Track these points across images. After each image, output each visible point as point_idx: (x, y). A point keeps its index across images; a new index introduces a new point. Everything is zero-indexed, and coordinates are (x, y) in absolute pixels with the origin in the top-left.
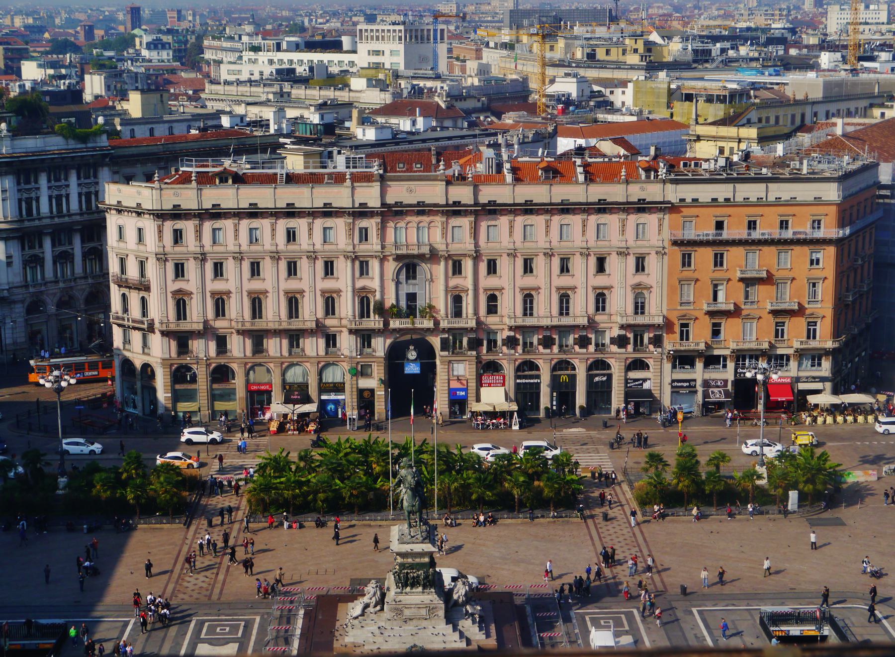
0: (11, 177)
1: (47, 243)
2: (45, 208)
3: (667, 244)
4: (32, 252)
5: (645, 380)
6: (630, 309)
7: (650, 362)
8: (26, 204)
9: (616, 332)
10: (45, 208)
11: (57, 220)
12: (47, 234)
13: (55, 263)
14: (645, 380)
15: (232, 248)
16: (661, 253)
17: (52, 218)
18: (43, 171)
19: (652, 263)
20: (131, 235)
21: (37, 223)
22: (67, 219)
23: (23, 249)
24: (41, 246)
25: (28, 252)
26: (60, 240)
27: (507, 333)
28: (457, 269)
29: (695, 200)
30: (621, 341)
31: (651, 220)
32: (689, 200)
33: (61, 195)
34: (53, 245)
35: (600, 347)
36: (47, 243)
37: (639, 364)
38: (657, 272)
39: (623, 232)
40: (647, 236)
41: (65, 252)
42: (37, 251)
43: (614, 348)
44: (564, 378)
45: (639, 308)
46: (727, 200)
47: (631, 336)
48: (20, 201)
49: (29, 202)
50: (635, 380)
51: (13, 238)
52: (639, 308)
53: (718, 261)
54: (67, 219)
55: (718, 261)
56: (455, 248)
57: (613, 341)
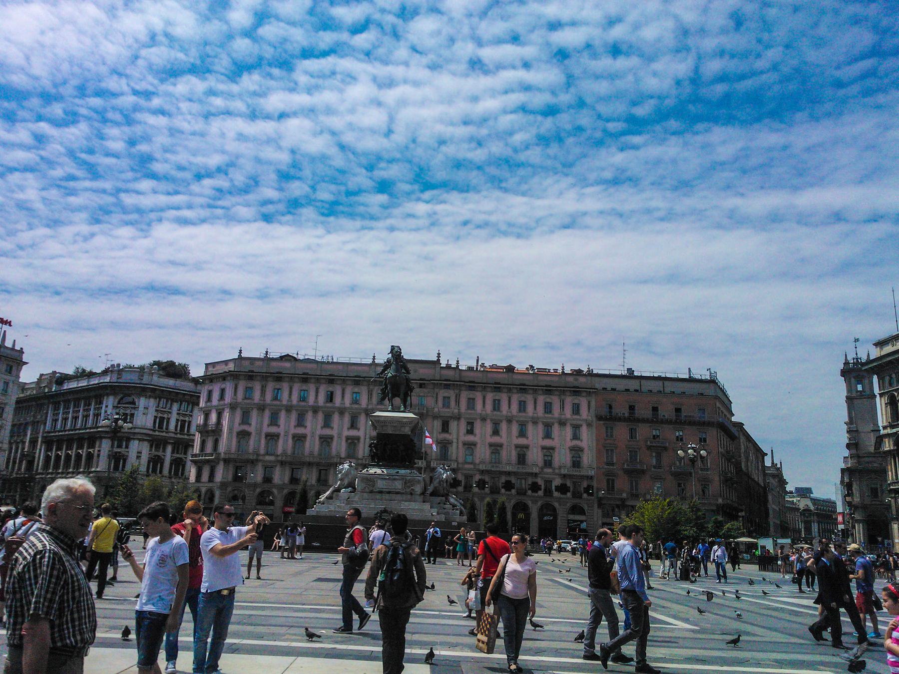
0: (152, 400)
1: (169, 449)
2: (172, 427)
3: (594, 419)
4: (157, 453)
5: (582, 522)
6: (569, 463)
7: (586, 508)
8: (161, 422)
9: (557, 482)
10: (172, 427)
11: (179, 436)
12: (170, 443)
13: (171, 464)
14: (582, 522)
15: (285, 402)
16: (589, 425)
17: (176, 434)
18: (177, 402)
19: (584, 432)
20: (216, 396)
21: (164, 434)
22: (186, 437)
23: (151, 450)
24: (164, 451)
25: (154, 452)
26: (178, 448)
27: (477, 477)
28: (445, 428)
29: (614, 390)
30: (563, 489)
31: (583, 402)
32: (609, 389)
33: (185, 421)
34: (173, 452)
35: (548, 492)
36: (169, 449)
37: (576, 509)
38: (587, 439)
39: (562, 407)
40: (581, 412)
41: (181, 459)
42: (160, 453)
43: (556, 494)
44: (521, 516)
45: (576, 464)
46: (636, 391)
47: (569, 484)
48: (156, 417)
49: (162, 419)
50: (575, 521)
51: (144, 440)
52: (576, 464)
53: (632, 432)
54: (186, 437)
55: (632, 432)
56: (446, 412)
57: (558, 489)
